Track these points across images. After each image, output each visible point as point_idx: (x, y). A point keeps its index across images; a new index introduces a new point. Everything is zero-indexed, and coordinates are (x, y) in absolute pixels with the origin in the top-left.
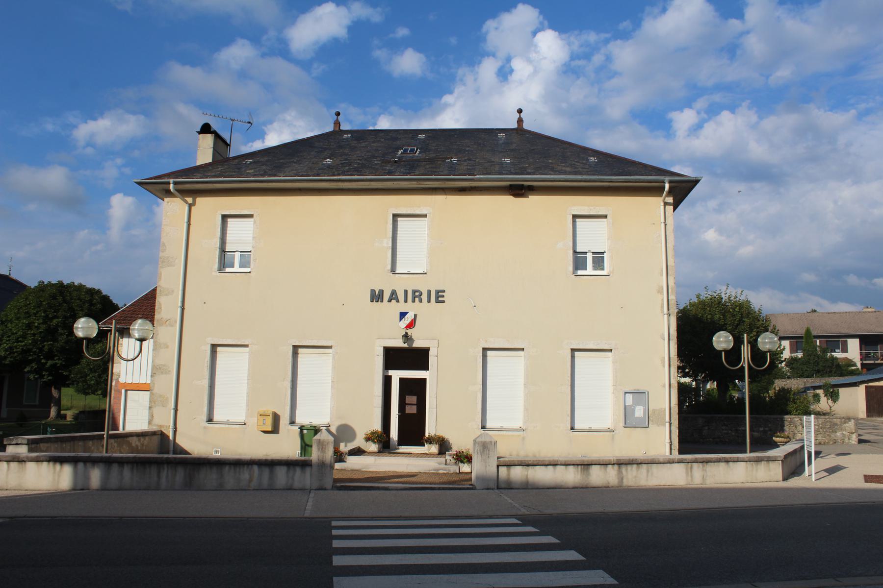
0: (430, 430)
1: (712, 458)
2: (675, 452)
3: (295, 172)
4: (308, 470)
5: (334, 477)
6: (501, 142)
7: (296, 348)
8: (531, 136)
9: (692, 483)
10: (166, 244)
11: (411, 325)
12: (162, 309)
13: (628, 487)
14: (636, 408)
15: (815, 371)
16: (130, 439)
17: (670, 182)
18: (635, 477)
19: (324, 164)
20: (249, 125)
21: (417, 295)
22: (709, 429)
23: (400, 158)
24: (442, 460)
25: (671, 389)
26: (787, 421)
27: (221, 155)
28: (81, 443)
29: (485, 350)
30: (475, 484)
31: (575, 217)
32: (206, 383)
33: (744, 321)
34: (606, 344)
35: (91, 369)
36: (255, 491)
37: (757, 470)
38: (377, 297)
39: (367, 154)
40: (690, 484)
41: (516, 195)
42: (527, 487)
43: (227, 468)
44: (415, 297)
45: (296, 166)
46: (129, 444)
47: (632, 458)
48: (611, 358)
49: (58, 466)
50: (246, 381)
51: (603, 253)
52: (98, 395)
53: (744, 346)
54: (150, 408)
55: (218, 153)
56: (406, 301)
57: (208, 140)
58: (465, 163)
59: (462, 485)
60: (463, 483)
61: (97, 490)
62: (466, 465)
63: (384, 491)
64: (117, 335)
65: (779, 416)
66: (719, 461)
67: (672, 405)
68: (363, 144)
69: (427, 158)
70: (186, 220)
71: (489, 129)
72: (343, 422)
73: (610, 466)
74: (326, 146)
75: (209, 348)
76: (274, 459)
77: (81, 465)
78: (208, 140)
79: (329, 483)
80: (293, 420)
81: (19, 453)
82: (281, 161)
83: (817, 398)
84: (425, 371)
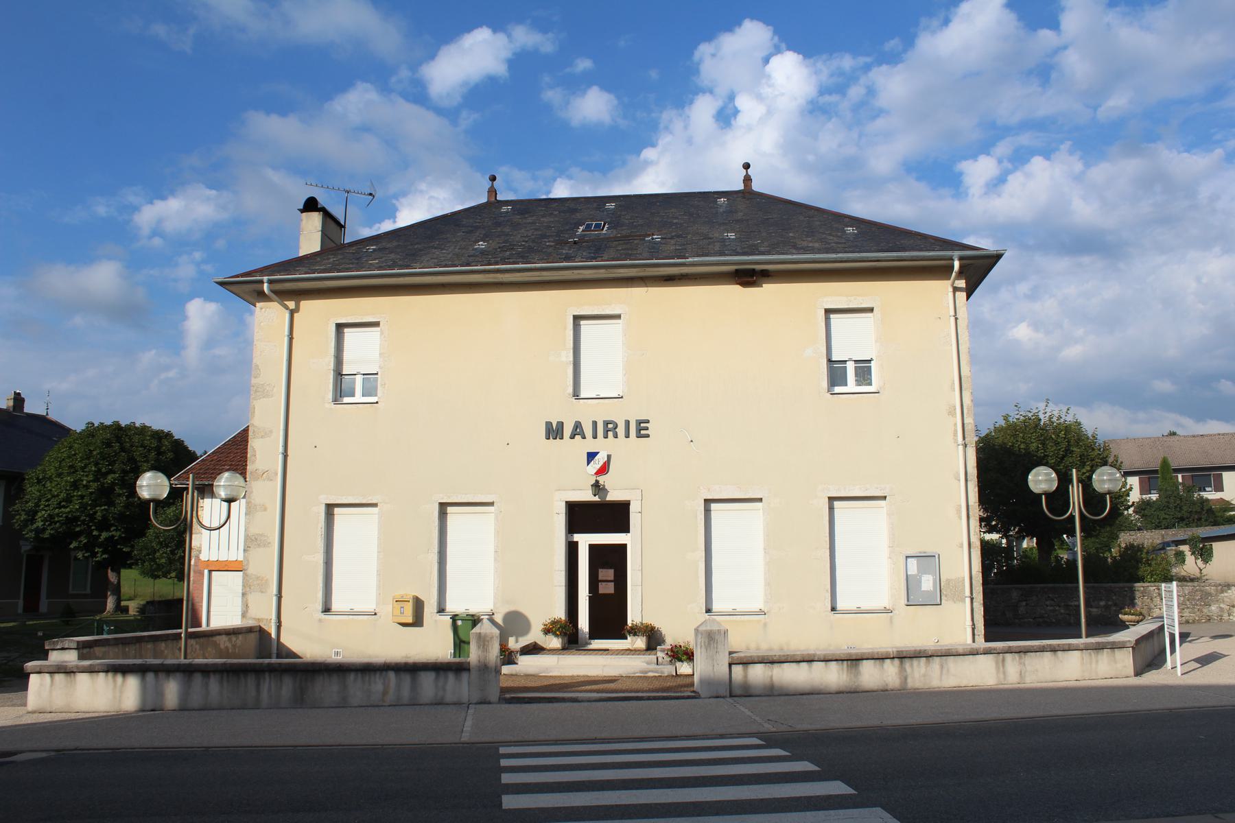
0: (634, 616)
3: (436, 261)
4: (465, 675)
5: (501, 685)
6: (721, 210)
7: (443, 507)
9: (1006, 682)
11: (603, 470)
13: (915, 689)
15: (1177, 518)
16: (217, 638)
17: (961, 259)
18: (924, 675)
19: (476, 249)
20: (371, 197)
21: (610, 428)
22: (1027, 605)
23: (582, 237)
24: (652, 658)
25: (972, 550)
26: (1138, 591)
27: (333, 242)
28: (150, 646)
30: (699, 691)
31: (828, 312)
32: (320, 558)
35: (161, 543)
37: (1097, 662)
38: (554, 432)
40: (1002, 684)
42: (772, 692)
43: (352, 676)
44: (608, 431)
46: (216, 645)
48: (885, 508)
49: (119, 678)
51: (869, 361)
52: (171, 578)
53: (1073, 486)
54: (243, 594)
56: (595, 437)
57: (314, 221)
58: (673, 242)
59: (681, 692)
62: (685, 664)
63: (571, 704)
64: (196, 494)
65: (1128, 585)
66: (1042, 650)
67: (973, 573)
68: (530, 220)
69: (619, 235)
71: (704, 193)
72: (512, 608)
74: (477, 224)
75: (322, 509)
76: (417, 661)
77: (150, 677)
78: (314, 221)
79: (494, 695)
80: (442, 607)
81: (66, 662)
82: (416, 247)
83: (1180, 557)
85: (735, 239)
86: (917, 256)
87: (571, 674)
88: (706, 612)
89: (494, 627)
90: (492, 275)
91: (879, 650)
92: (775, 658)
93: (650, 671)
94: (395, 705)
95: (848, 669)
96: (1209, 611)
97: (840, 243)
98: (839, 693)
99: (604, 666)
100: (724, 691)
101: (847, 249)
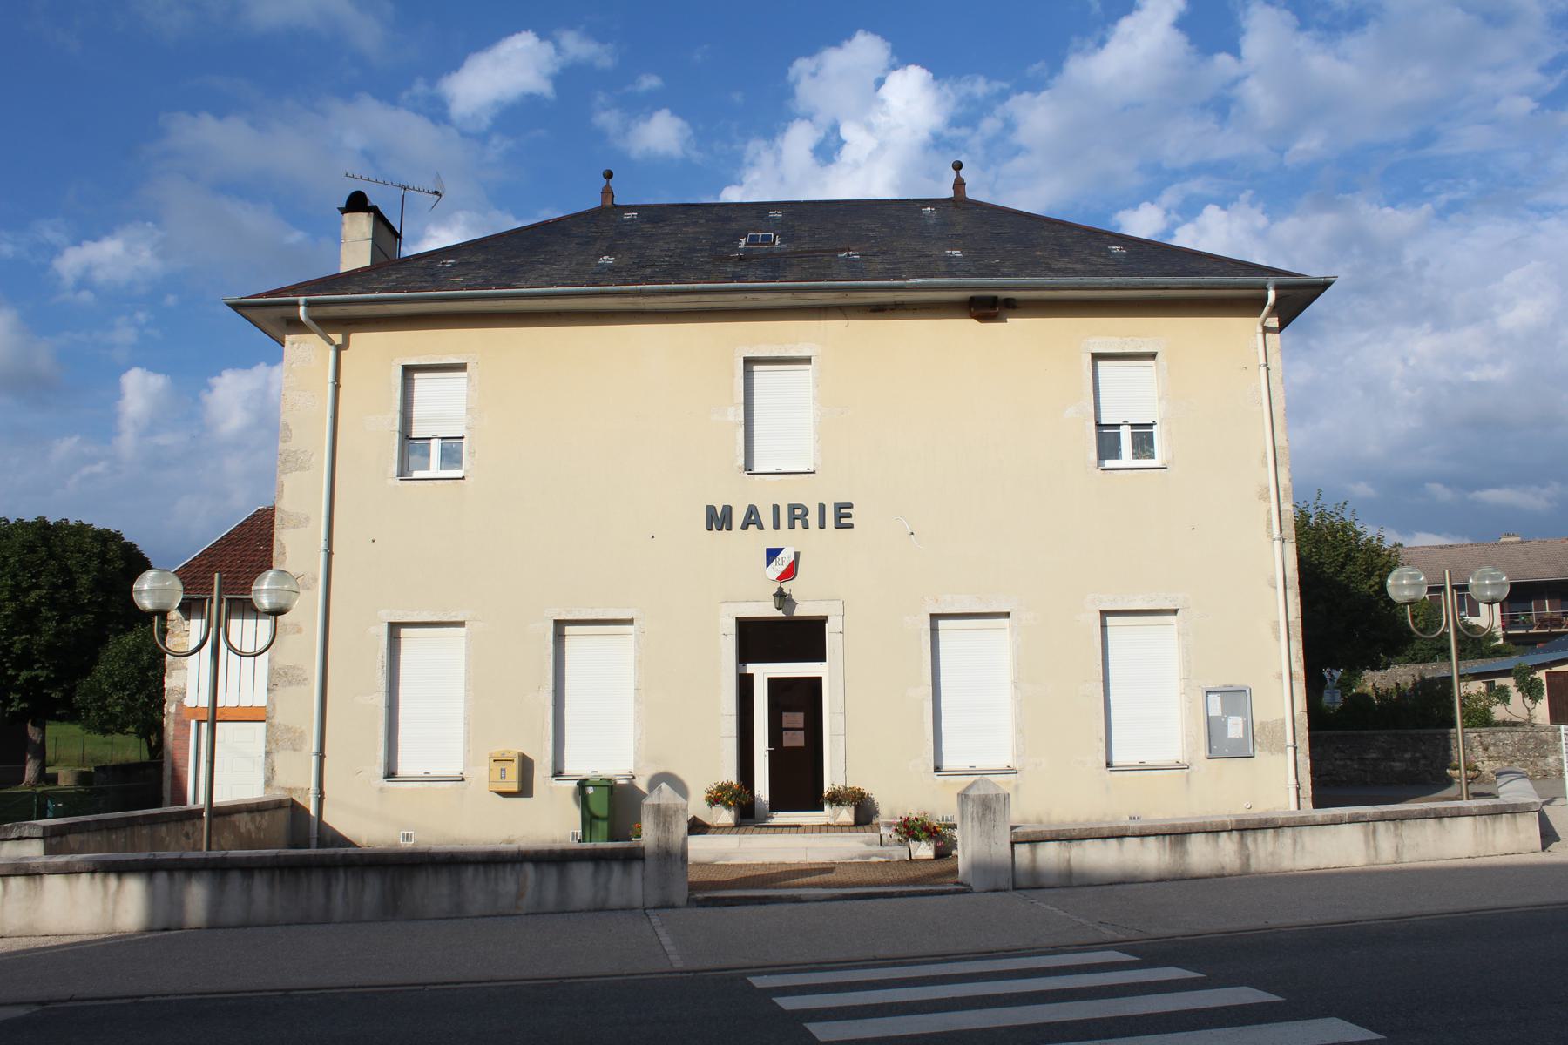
0: (833, 777)
1: (1412, 811)
2: (1307, 803)
3: (547, 279)
4: (637, 868)
5: (690, 879)
6: (932, 222)
7: (560, 625)
8: (985, 211)
9: (1378, 862)
10: (290, 427)
11: (789, 573)
12: (287, 554)
13: (1260, 873)
14: (1230, 722)
15: (1437, 649)
16: (236, 818)
17: (1277, 287)
18: (1272, 854)
19: (601, 265)
20: (436, 197)
21: (798, 514)
23: (745, 251)
27: (386, 255)
29: (935, 617)
30: (969, 880)
31: (1097, 357)
32: (380, 700)
33: (1354, 557)
34: (1166, 598)
35: (114, 685)
36: (530, 917)
37: (1494, 831)
38: (719, 519)
39: (680, 246)
41: (984, 317)
42: (1072, 882)
43: (469, 872)
44: (794, 519)
45: (547, 269)
46: (235, 828)
47: (1264, 817)
48: (1176, 627)
49: (112, 881)
50: (462, 693)
51: (1150, 426)
52: (128, 733)
53: (1445, 594)
54: (268, 754)
55: (381, 249)
56: (777, 527)
57: (359, 227)
58: (878, 259)
60: (937, 880)
61: (199, 928)
62: (923, 844)
65: (1442, 731)
66: (1424, 815)
67: (1297, 713)
68: (667, 230)
70: (330, 377)
73: (1224, 834)
74: (594, 234)
75: (384, 631)
77: (161, 878)
78: (359, 227)
79: (680, 895)
81: (27, 858)
82: (513, 261)
83: (1503, 694)
84: (818, 663)
85: (964, 257)
86: (1220, 283)
87: (761, 862)
88: (935, 771)
89: (677, 795)
90: (631, 299)
91: (1212, 820)
92: (1074, 834)
93: (873, 856)
94: (532, 914)
95: (1171, 849)
96: (1545, 764)
97: (1109, 265)
98: (1160, 880)
99: (807, 848)
100: (1004, 881)
101: (1120, 272)
